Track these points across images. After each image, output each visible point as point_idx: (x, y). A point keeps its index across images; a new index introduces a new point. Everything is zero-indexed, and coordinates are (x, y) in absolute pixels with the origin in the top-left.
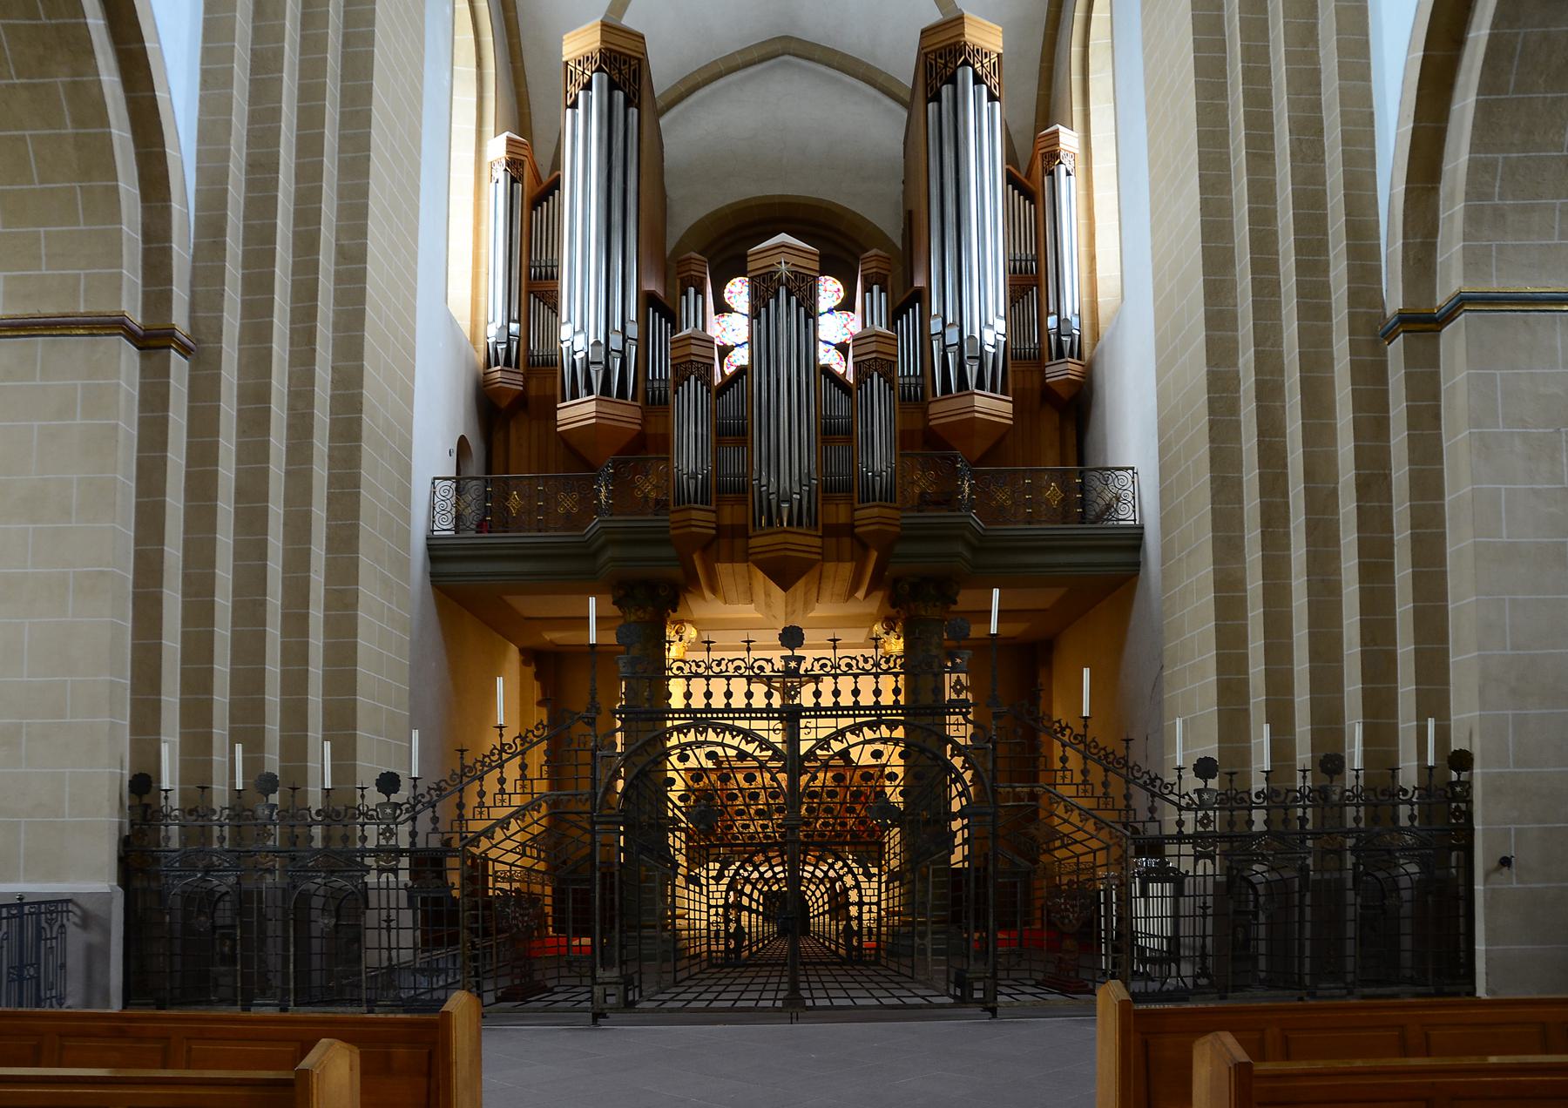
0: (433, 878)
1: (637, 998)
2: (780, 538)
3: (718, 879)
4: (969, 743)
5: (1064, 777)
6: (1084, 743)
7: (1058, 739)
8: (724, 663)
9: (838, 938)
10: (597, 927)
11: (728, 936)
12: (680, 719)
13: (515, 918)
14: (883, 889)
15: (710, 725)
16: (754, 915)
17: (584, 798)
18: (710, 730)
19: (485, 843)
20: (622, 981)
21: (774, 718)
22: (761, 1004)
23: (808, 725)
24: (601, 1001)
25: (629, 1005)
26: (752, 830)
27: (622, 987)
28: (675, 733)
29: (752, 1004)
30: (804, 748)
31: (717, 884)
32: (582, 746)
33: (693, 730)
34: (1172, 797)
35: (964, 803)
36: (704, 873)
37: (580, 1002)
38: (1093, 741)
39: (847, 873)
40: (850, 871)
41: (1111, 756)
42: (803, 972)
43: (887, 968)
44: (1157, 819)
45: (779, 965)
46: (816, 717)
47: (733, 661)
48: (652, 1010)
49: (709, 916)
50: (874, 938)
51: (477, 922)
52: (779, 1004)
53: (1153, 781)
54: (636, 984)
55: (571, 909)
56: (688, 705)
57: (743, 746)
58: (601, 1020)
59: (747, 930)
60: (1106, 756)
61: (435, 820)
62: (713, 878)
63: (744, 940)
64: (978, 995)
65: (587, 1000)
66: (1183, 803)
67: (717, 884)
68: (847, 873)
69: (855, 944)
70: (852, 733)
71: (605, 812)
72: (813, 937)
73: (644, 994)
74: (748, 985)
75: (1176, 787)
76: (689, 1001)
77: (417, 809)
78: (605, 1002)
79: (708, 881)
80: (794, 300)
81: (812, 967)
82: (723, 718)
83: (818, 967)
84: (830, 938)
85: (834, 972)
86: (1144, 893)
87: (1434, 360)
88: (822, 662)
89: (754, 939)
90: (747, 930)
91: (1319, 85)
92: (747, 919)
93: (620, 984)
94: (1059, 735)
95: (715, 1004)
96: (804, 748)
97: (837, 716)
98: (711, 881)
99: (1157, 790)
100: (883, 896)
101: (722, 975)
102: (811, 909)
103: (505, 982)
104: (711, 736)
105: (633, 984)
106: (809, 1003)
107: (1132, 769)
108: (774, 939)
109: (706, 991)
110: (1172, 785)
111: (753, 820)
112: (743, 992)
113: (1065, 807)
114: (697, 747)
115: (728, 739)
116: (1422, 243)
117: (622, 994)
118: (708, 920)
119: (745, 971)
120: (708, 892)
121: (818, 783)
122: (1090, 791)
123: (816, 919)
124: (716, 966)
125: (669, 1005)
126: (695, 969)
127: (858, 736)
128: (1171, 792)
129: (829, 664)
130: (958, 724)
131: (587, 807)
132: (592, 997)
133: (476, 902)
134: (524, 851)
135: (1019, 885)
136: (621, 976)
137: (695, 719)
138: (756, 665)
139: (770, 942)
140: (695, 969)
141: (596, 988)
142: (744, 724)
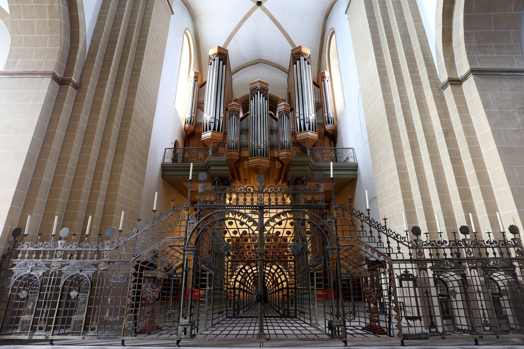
1: (196, 333)
2: (258, 159)
3: (231, 276)
5: (363, 234)
6: (369, 220)
7: (359, 218)
8: (236, 187)
10: (182, 298)
16: (245, 293)
17: (182, 239)
20: (190, 324)
25: (193, 336)
32: (183, 219)
34: (405, 243)
38: (372, 219)
39: (282, 274)
40: (283, 273)
41: (380, 225)
42: (265, 321)
44: (401, 252)
45: (255, 317)
50: (294, 305)
51: (134, 294)
52: (255, 336)
53: (397, 236)
54: (196, 325)
55: (172, 289)
57: (242, 220)
60: (378, 225)
62: (229, 275)
66: (410, 245)
67: (231, 278)
68: (282, 274)
69: (286, 308)
70: (283, 215)
71: (189, 246)
72: (269, 304)
73: (199, 331)
75: (406, 239)
79: (227, 277)
80: (262, 95)
81: (269, 319)
83: (271, 319)
84: (276, 305)
86: (401, 286)
87: (462, 93)
88: (271, 188)
89: (245, 305)
91: (406, 26)
92: (242, 295)
94: (359, 217)
96: (265, 220)
97: (277, 209)
98: (229, 277)
99: (399, 240)
102: (268, 291)
105: (194, 326)
106: (268, 337)
107: (389, 231)
109: (225, 330)
110: (405, 238)
113: (365, 246)
116: (450, 60)
122: (374, 240)
126: (220, 319)
128: (405, 241)
131: (183, 244)
133: (136, 285)
135: (350, 280)
136: (190, 322)
138: (248, 188)
139: (251, 306)
140: (220, 319)
142: (243, 211)
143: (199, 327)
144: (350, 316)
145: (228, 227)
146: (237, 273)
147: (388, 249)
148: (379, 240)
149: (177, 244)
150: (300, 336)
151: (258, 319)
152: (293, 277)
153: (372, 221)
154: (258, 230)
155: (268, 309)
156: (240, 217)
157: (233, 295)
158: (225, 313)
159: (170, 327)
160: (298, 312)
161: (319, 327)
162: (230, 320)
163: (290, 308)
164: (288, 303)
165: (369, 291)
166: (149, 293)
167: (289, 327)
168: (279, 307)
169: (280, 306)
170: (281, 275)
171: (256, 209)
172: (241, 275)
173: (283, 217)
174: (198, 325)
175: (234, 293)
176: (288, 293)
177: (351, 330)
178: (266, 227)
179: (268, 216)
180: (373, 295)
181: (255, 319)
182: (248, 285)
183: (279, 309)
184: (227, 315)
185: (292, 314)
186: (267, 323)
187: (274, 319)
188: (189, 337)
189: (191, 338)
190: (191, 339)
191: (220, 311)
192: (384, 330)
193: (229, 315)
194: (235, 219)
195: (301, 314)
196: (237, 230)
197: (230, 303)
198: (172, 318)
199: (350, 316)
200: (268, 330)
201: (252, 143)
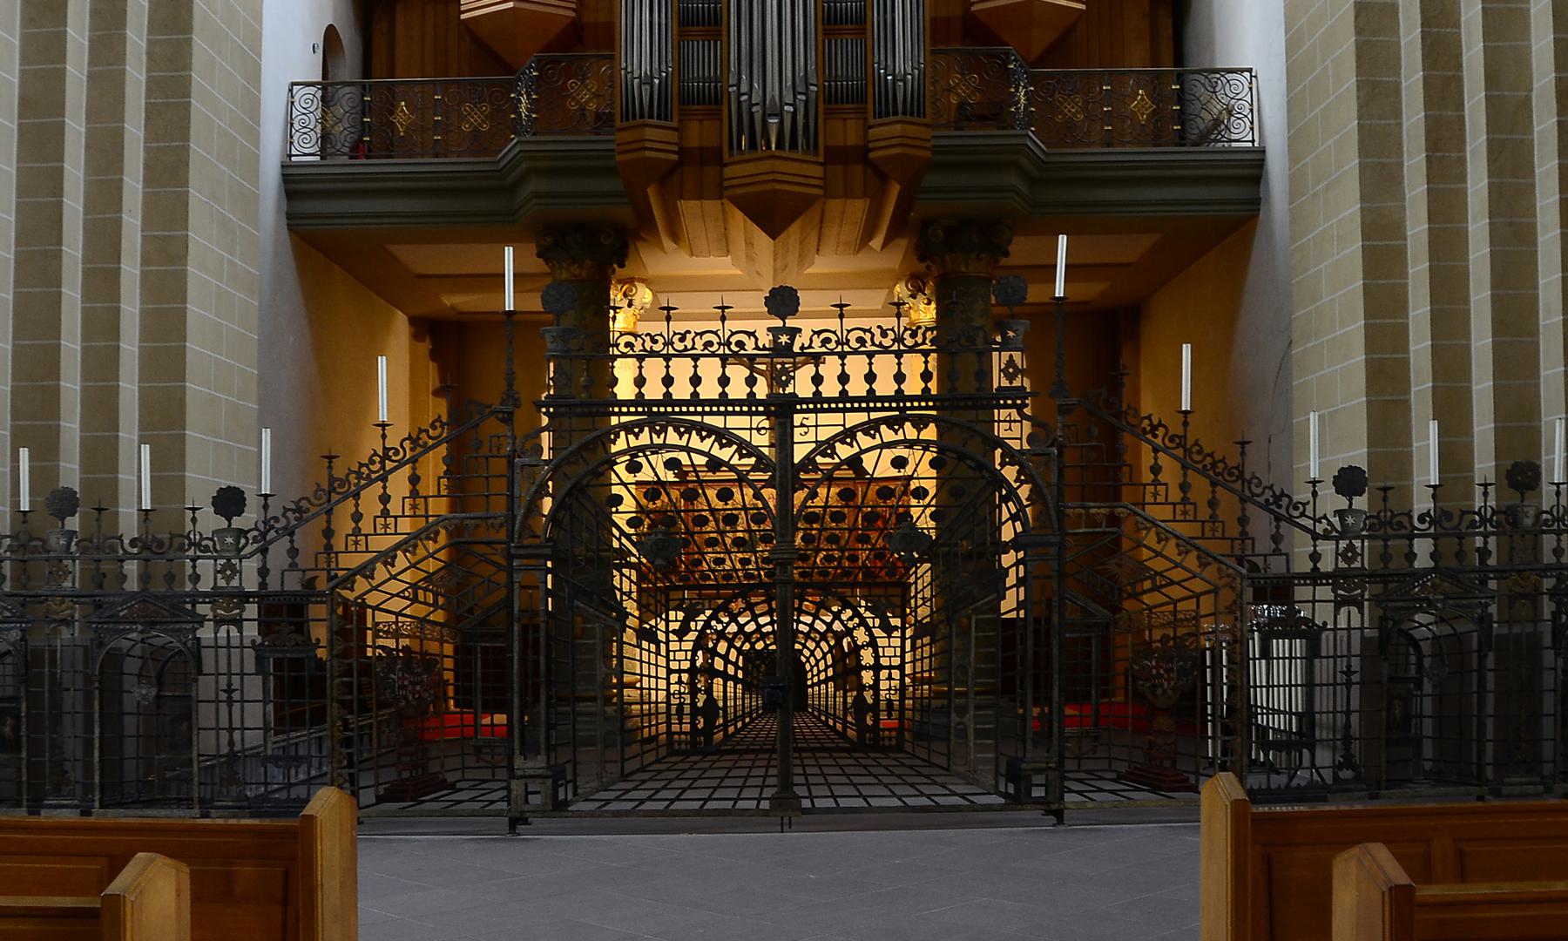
0: (291, 632)
1: (570, 797)
3: (682, 633)
4: (1026, 447)
5: (1155, 494)
8: (689, 337)
9: (845, 715)
10: (516, 700)
11: (695, 711)
12: (629, 413)
13: (402, 687)
14: (908, 648)
15: (669, 423)
16: (730, 684)
17: (498, 521)
18: (670, 429)
19: (361, 585)
20: (550, 773)
21: (758, 413)
22: (741, 805)
23: (805, 422)
24: (521, 801)
25: (559, 807)
26: (728, 565)
27: (549, 782)
28: (622, 434)
29: (729, 804)
30: (799, 453)
31: (681, 641)
33: (646, 429)
35: (1019, 529)
36: (662, 626)
37: (493, 802)
39: (859, 625)
40: (863, 622)
41: (1221, 465)
42: (797, 762)
45: (765, 751)
46: (815, 411)
47: (701, 334)
48: (590, 814)
49: (669, 684)
50: (895, 714)
52: (765, 805)
53: (1277, 499)
54: (569, 778)
55: (479, 675)
56: (640, 395)
57: (716, 451)
58: (520, 828)
59: (721, 704)
60: (1214, 465)
61: (293, 552)
62: (674, 632)
63: (717, 717)
64: (1038, 792)
65: (501, 800)
66: (1320, 529)
67: (681, 641)
68: (859, 625)
69: (870, 722)
71: (526, 542)
72: (812, 714)
73: (580, 791)
74: (722, 779)
75: (1309, 508)
76: (642, 802)
77: (269, 537)
78: (527, 802)
79: (667, 637)
83: (817, 755)
84: (834, 715)
85: (841, 762)
86: (1266, 653)
90: (721, 704)
93: (548, 777)
94: (1149, 436)
95: (677, 805)
96: (799, 453)
97: (844, 410)
98: (672, 637)
99: (1283, 511)
100: (908, 657)
102: (809, 675)
103: (389, 775)
104: (672, 437)
105: (564, 777)
106: (806, 803)
107: (1250, 483)
108: (759, 716)
109: (664, 788)
111: (729, 553)
112: (715, 789)
114: (653, 453)
115: (695, 442)
117: (550, 792)
118: (668, 690)
119: (718, 760)
120: (668, 651)
121: (819, 502)
122: (1191, 513)
123: (816, 688)
124: (678, 753)
125: (614, 806)
126: (650, 757)
127: (874, 438)
128: (1303, 514)
129: (834, 338)
130: (1010, 421)
134: (416, 595)
135: (1094, 642)
136: (549, 767)
137: (650, 413)
138: (734, 340)
139: (752, 720)
140: (650, 757)
141: (514, 783)
147: (1237, 543)
148: (1210, 512)
151: (774, 756)
152: (895, 634)
153: (1195, 449)
156: (709, 441)
162: (682, 761)
165: (1154, 671)
166: (402, 687)
169: (849, 719)
170: (854, 628)
173: (864, 441)
177: (1080, 781)
179: (811, 437)
180: (1166, 684)
181: (767, 756)
189: (554, 810)
192: (1187, 780)
193: (676, 747)
198: (489, 758)
201: (738, 85)
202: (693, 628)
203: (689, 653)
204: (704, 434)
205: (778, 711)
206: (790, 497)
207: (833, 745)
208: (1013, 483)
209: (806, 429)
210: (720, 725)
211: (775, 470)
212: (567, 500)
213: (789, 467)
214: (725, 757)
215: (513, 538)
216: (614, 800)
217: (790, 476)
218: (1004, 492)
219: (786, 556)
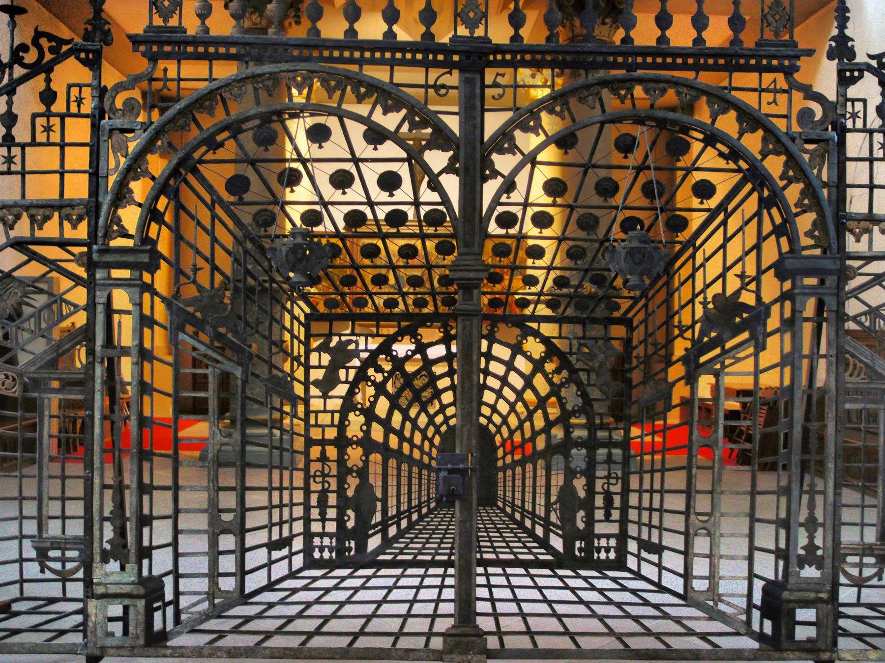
1: (170, 626)
3: (328, 384)
4: (796, 128)
9: (548, 512)
16: (392, 463)
20: (141, 591)
21: (436, 64)
22: (404, 643)
23: (500, 80)
31: (325, 396)
35: (785, 248)
36: (300, 373)
37: (62, 632)
42: (481, 580)
43: (638, 576)
49: (308, 462)
50: (616, 515)
52: (437, 643)
54: (169, 596)
57: (378, 117)
59: (379, 494)
62: (316, 383)
63: (374, 512)
64: (802, 633)
65: (74, 630)
67: (325, 396)
69: (581, 525)
72: (503, 510)
73: (183, 617)
76: (268, 635)
79: (307, 390)
81: (499, 570)
82: (342, 60)
83: (509, 571)
84: (533, 513)
85: (541, 582)
89: (392, 512)
90: (379, 494)
92: (379, 469)
93: (138, 597)
95: (317, 642)
96: (493, 123)
98: (314, 391)
101: (330, 583)
102: (500, 452)
105: (162, 597)
108: (430, 511)
111: (394, 268)
119: (374, 576)
120: (308, 412)
121: (517, 196)
125: (230, 641)
126: (280, 570)
130: (775, 91)
132: (84, 623)
136: (142, 581)
139: (421, 518)
141: (93, 606)
142: (381, 74)
143: (184, 602)
144: (861, 565)
145: (305, 154)
146: (352, 373)
149: (51, 229)
150: (636, 643)
151: (451, 571)
154: (456, 172)
155: (498, 530)
157: (334, 472)
158: (298, 544)
159: (52, 601)
160: (632, 546)
161: (722, 607)
162: (324, 577)
163: (599, 528)
164: (588, 505)
167: (587, 604)
168: (547, 526)
169: (553, 518)
171: (449, 66)
172: (374, 383)
174: (177, 593)
175: (341, 461)
176: (592, 464)
177: (860, 619)
178: (495, 157)
181: (440, 571)
182: (408, 425)
183: (547, 532)
184: (308, 550)
185: (608, 550)
186: (490, 586)
187: (522, 571)
188: (142, 641)
190: (151, 651)
191: (275, 537)
193: (317, 555)
194: (342, 116)
195: (644, 554)
196: (349, 167)
197: (323, 505)
198: (57, 566)
199: (861, 565)
200: (496, 615)
202: (343, 378)
203: (337, 416)
204: (363, 90)
205: (457, 504)
206: (478, 189)
207: (531, 557)
208: (778, 181)
209: (500, 91)
210: (376, 525)
211: (458, 148)
212: (172, 182)
213: (478, 144)
214: (383, 572)
215: (96, 235)
216: (230, 632)
217: (478, 157)
218: (766, 193)
219: (472, 275)
